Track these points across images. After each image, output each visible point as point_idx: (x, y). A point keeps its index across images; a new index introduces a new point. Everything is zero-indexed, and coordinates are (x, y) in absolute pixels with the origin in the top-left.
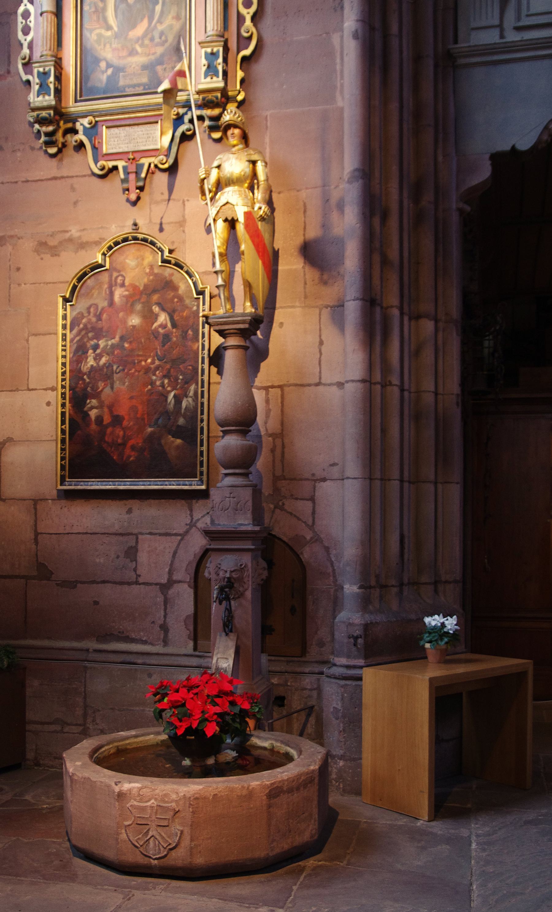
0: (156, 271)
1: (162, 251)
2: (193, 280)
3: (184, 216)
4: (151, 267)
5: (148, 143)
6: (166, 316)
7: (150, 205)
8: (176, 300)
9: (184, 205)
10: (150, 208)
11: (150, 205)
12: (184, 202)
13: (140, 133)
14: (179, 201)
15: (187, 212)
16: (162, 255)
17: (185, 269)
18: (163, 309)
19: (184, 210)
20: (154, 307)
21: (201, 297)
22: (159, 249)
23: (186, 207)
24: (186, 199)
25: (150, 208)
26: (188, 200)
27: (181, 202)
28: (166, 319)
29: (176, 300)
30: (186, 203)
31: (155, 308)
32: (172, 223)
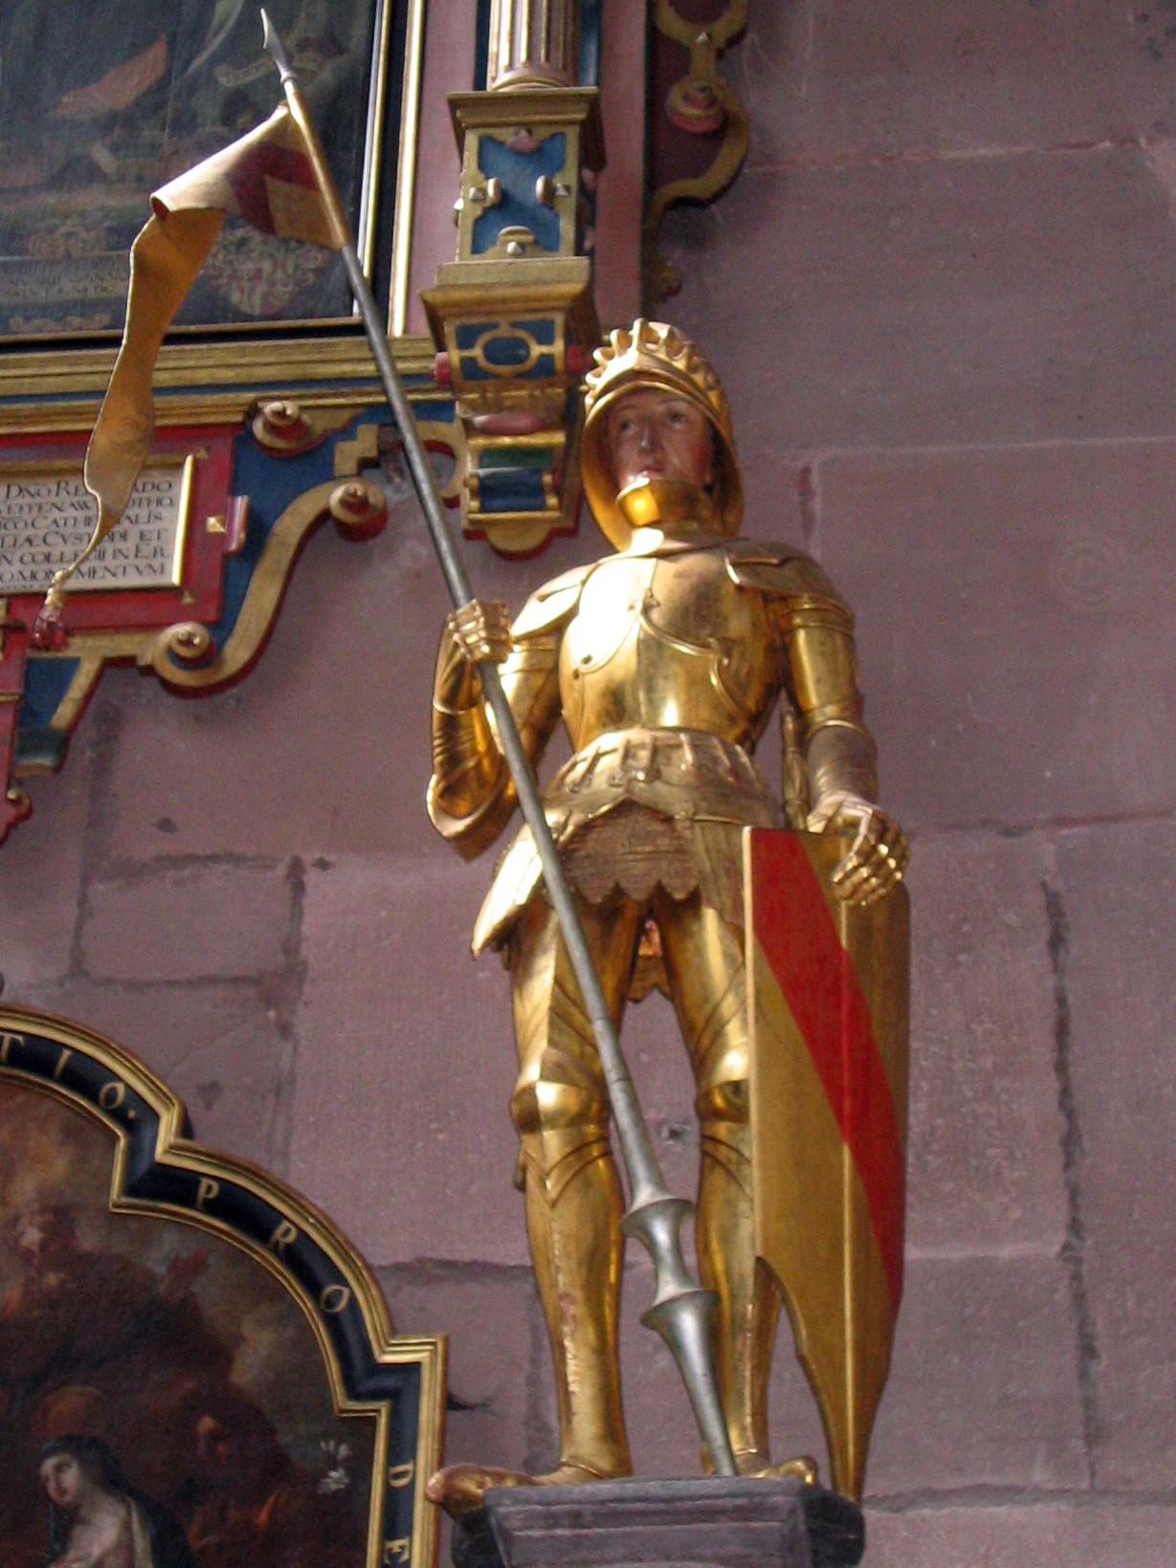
0: (88, 1240)
1: (137, 1120)
2: (325, 1306)
3: (291, 947)
4: (59, 1218)
5: (109, 561)
6: (127, 1526)
7: (86, 881)
8: (207, 1423)
9: (299, 887)
10: (83, 901)
11: (86, 881)
12: (296, 868)
13: (71, 512)
14: (266, 864)
15: (310, 926)
16: (132, 1153)
17: (284, 1234)
18: (113, 1480)
19: (297, 913)
20: (49, 1465)
21: (383, 1407)
22: (119, 1115)
23: (309, 901)
24: (309, 857)
25: (83, 901)
26: (323, 865)
27: (282, 870)
28: (126, 1545)
29: (207, 1423)
30: (311, 877)
31: (59, 1469)
32: (213, 980)
